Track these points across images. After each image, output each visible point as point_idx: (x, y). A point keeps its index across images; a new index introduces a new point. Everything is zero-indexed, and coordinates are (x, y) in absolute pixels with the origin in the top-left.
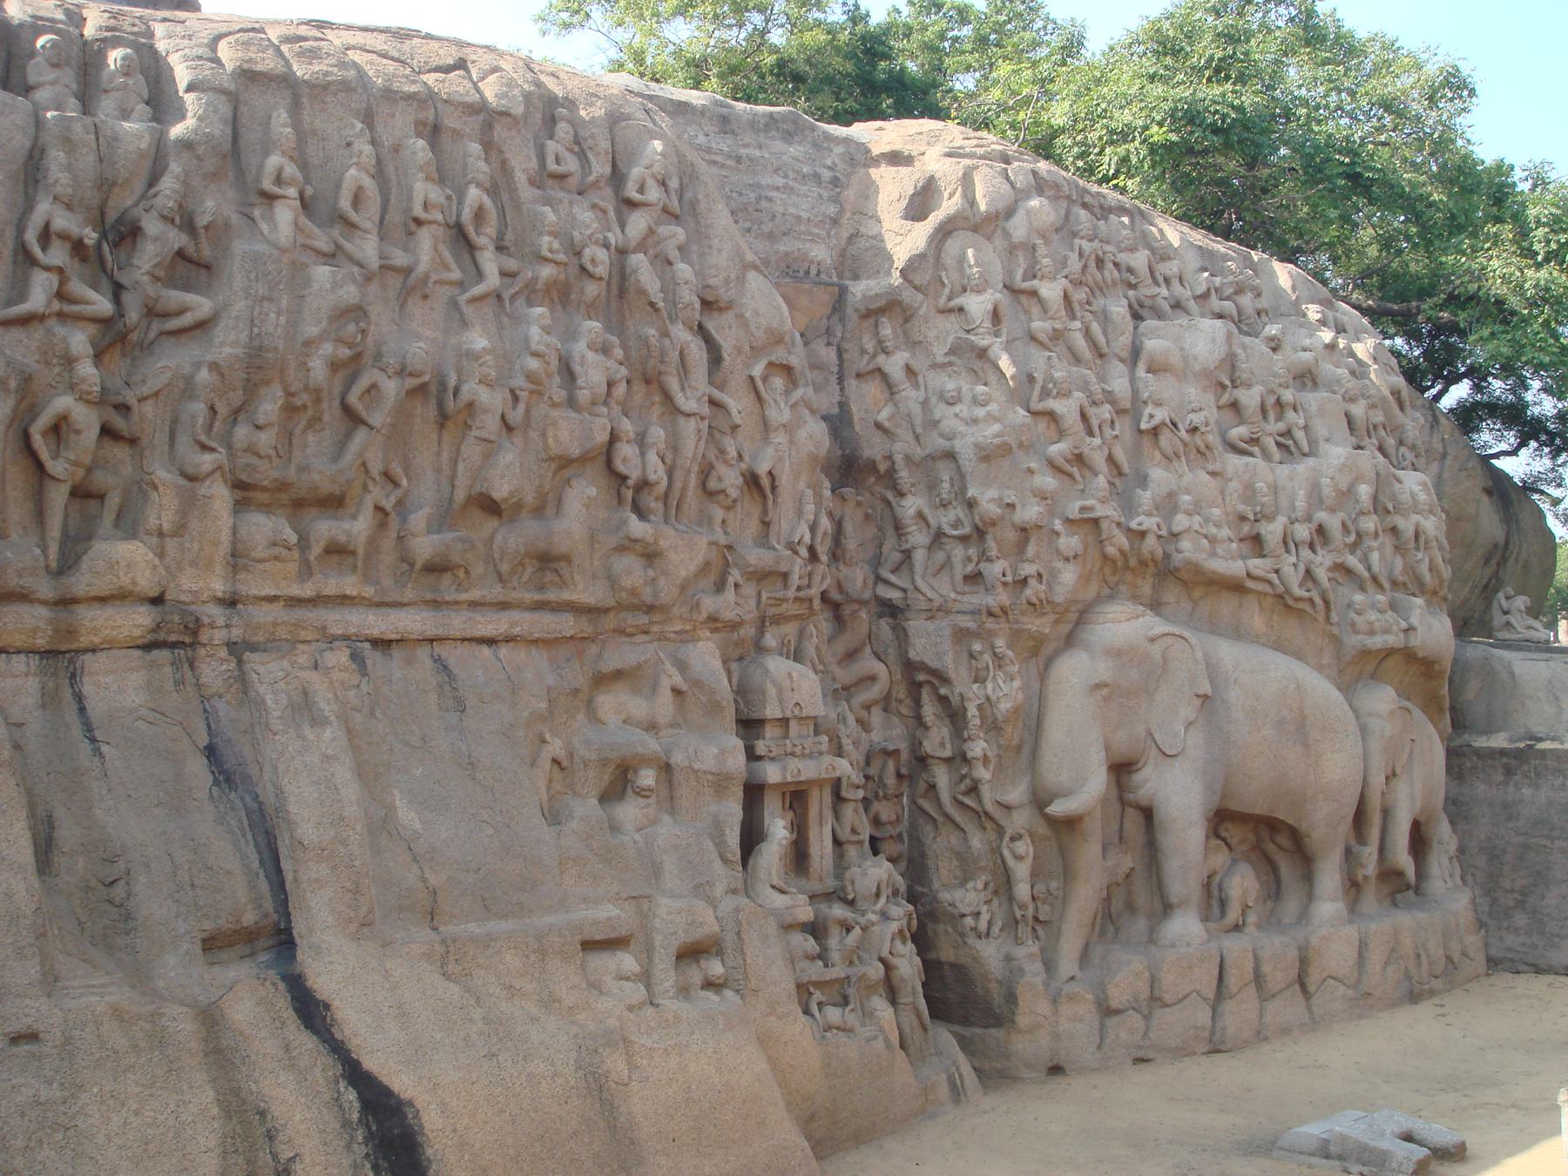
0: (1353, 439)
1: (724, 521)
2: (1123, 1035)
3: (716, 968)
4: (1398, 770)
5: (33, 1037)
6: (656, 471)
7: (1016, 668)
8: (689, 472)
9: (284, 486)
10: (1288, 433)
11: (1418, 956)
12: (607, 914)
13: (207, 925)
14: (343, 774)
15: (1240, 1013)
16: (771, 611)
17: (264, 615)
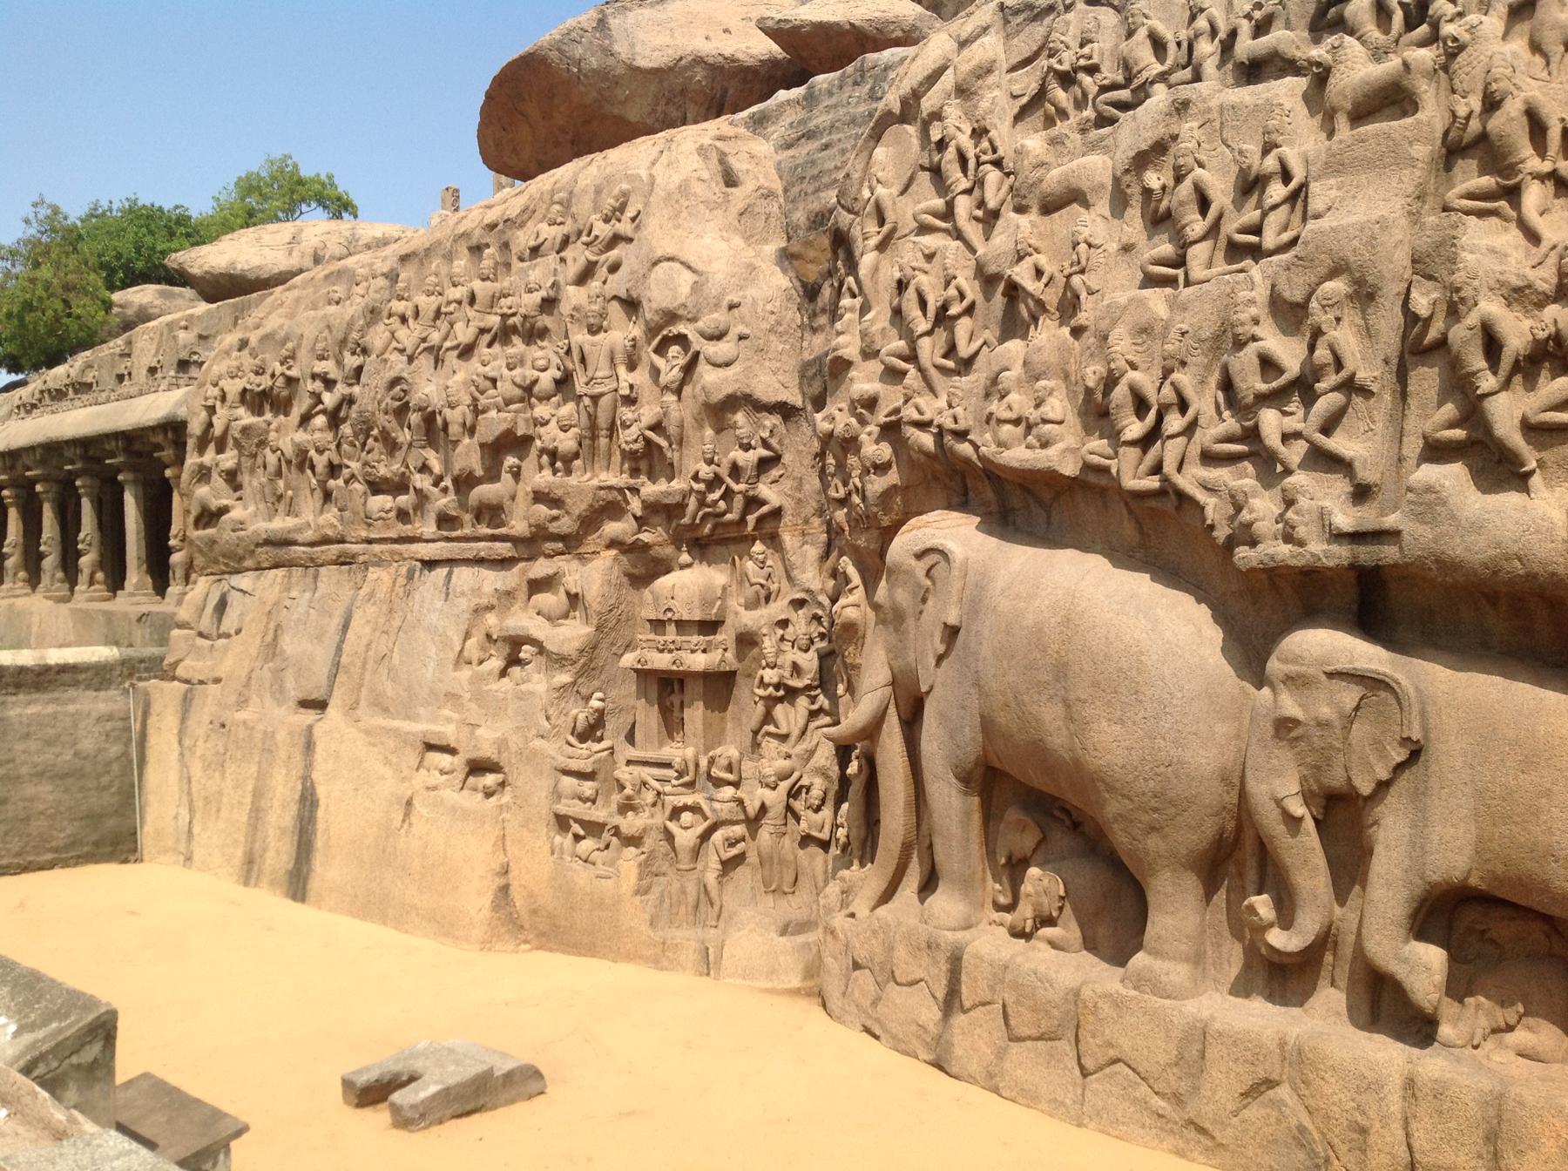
0: (1488, 182)
1: (635, 472)
2: (857, 993)
3: (490, 779)
4: (1365, 787)
5: (223, 726)
6: (567, 442)
7: (856, 579)
8: (594, 438)
9: (386, 480)
10: (1257, 230)
11: (1363, 1131)
12: (448, 731)
13: (302, 696)
14: (368, 630)
15: (974, 1035)
16: (688, 535)
17: (377, 548)
